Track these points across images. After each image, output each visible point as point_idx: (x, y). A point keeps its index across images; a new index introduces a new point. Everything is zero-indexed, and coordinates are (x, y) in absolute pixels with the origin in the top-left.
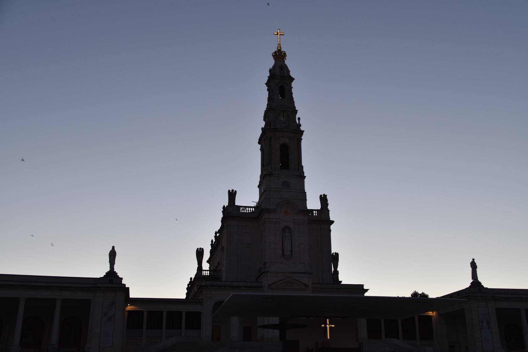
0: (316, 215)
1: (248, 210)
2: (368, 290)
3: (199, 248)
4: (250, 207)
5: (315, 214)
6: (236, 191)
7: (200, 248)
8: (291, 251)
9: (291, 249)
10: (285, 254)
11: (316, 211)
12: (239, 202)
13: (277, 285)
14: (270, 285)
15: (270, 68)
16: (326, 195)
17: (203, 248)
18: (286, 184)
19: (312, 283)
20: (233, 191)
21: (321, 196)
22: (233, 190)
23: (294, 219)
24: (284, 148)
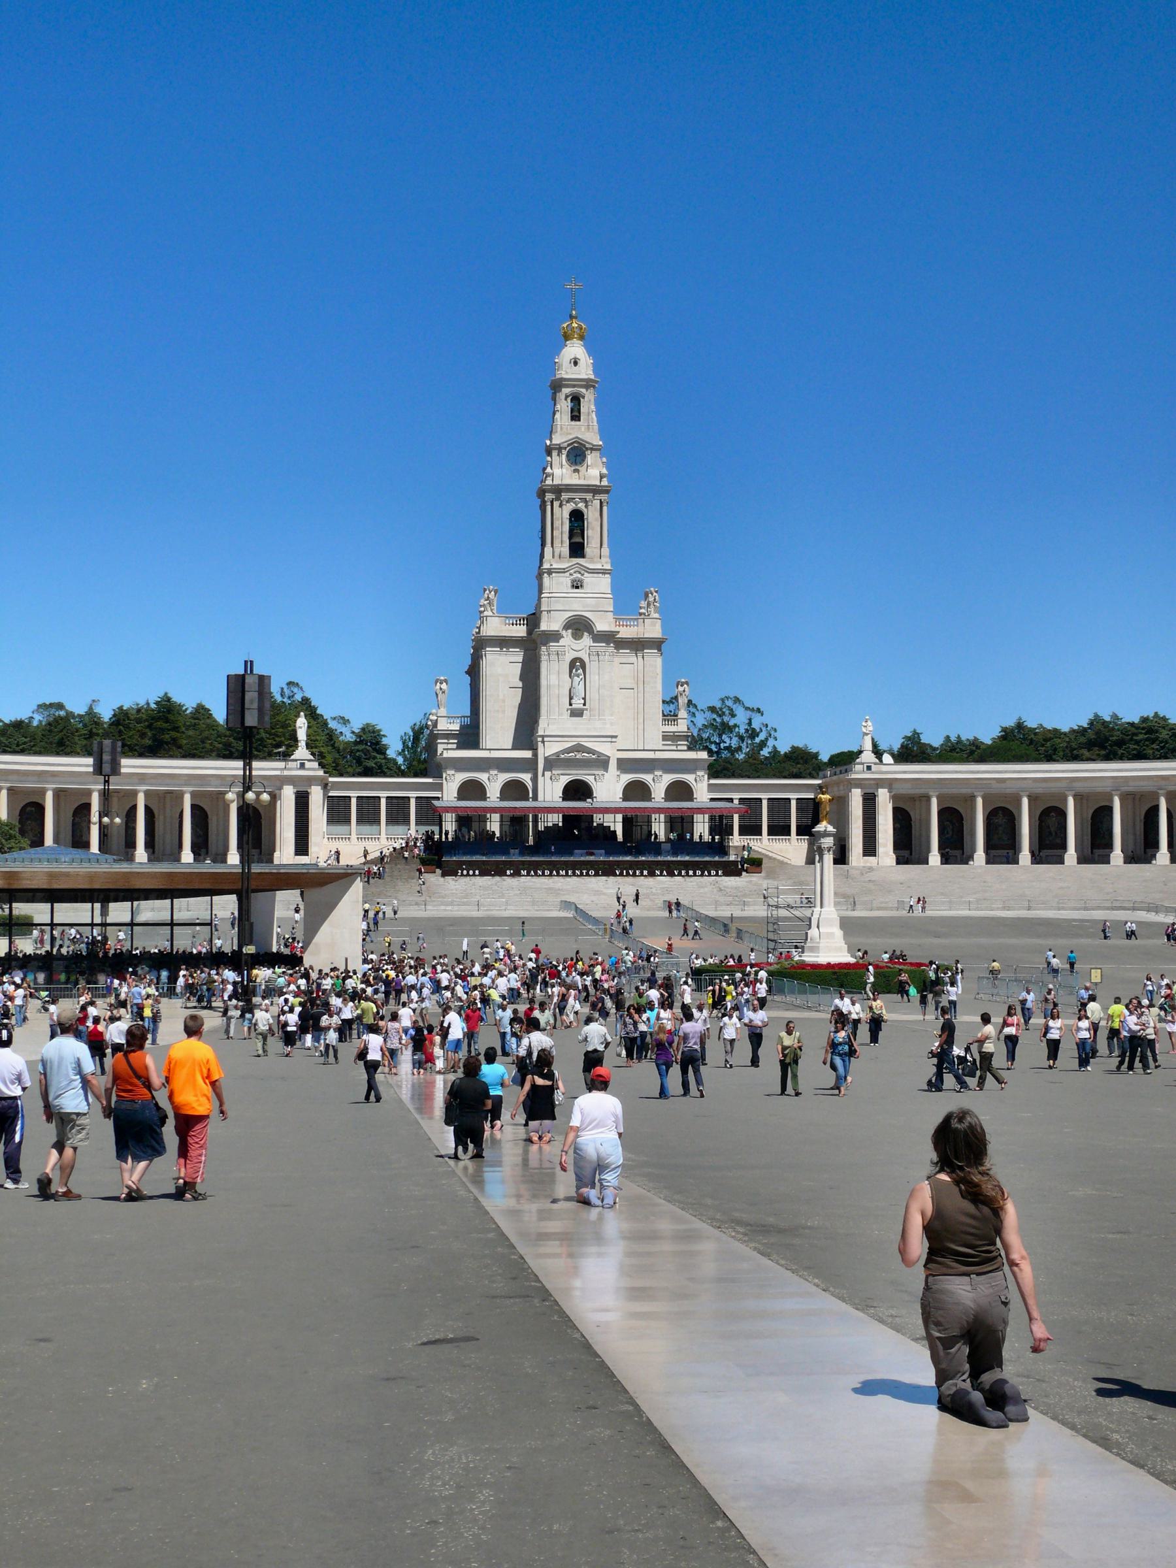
8: (584, 699)
18: (577, 585)
24: (577, 517)
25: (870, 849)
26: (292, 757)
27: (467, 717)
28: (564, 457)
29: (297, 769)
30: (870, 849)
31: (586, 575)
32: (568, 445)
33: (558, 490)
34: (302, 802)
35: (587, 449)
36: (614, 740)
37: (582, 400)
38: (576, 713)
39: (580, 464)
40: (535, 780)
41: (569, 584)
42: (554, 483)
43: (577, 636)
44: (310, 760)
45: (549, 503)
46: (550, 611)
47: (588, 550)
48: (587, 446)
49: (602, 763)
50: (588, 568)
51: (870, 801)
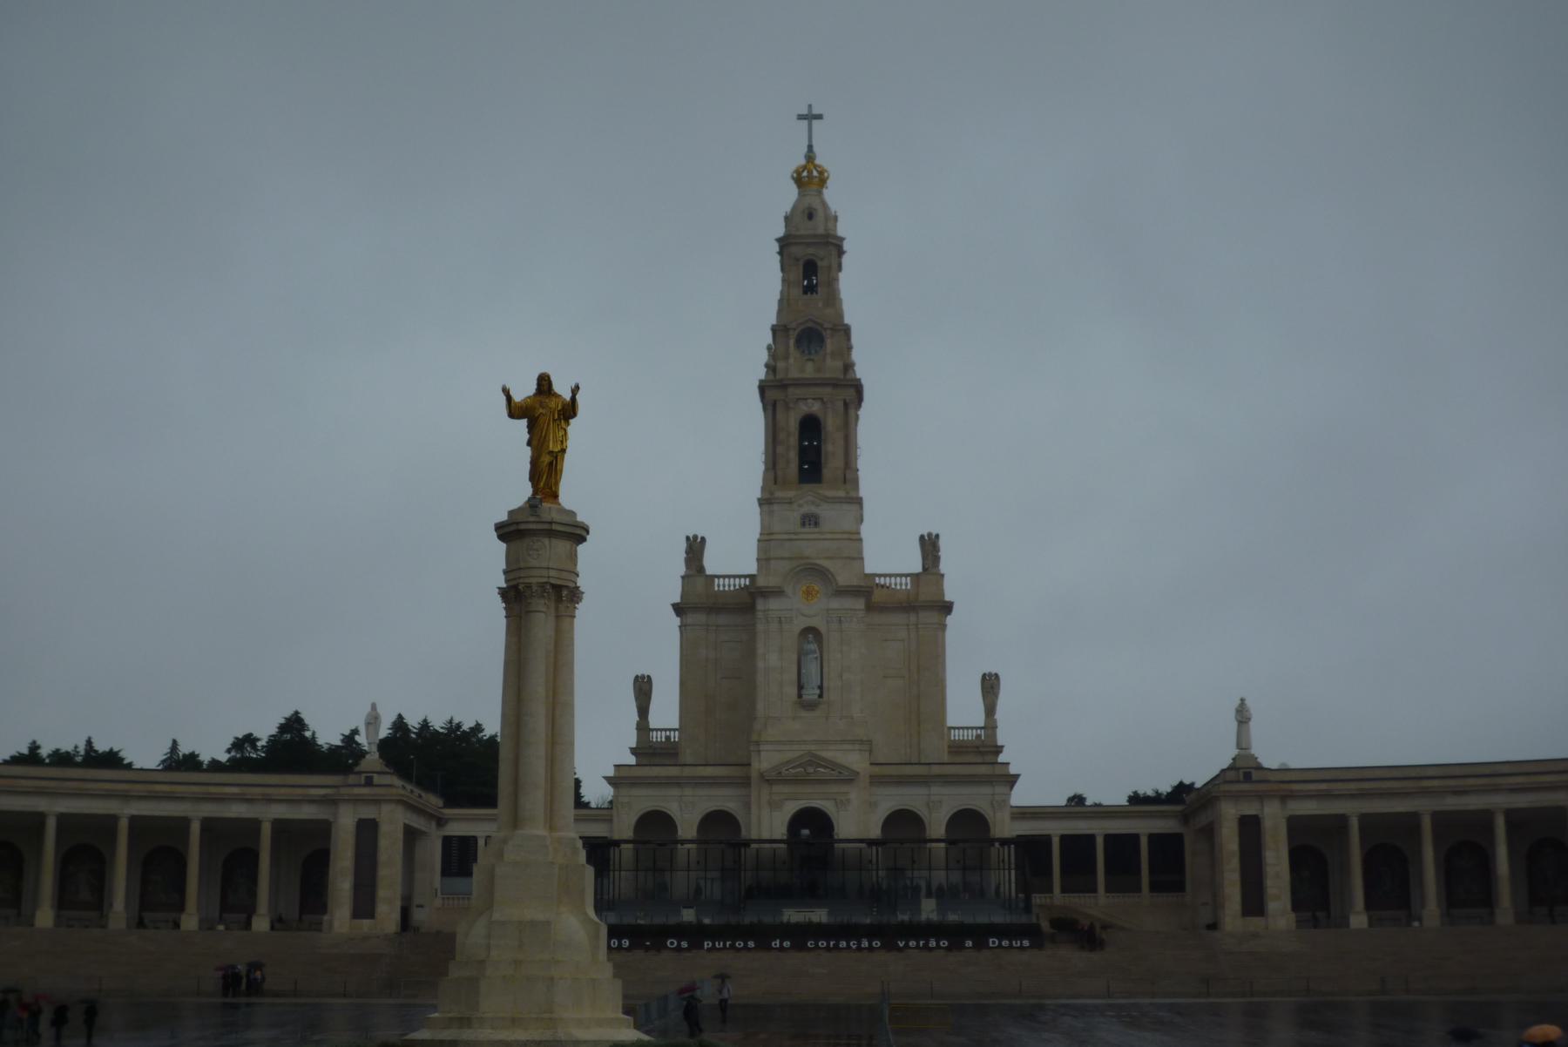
0: (909, 587)
1: (735, 586)
4: (740, 577)
5: (906, 584)
6: (703, 539)
7: (643, 677)
8: (821, 687)
9: (819, 683)
11: (909, 578)
12: (712, 564)
16: (937, 536)
17: (649, 677)
18: (810, 520)
21: (922, 537)
22: (695, 537)
23: (828, 610)
24: (811, 427)
25: (1254, 903)
26: (357, 769)
27: (675, 730)
28: (792, 342)
29: (359, 786)
30: (1254, 903)
33: (783, 386)
34: (367, 831)
35: (825, 329)
37: (819, 263)
38: (810, 706)
40: (747, 806)
42: (778, 377)
43: (809, 593)
44: (378, 773)
47: (827, 472)
48: (826, 325)
49: (849, 777)
50: (828, 498)
51: (1250, 828)
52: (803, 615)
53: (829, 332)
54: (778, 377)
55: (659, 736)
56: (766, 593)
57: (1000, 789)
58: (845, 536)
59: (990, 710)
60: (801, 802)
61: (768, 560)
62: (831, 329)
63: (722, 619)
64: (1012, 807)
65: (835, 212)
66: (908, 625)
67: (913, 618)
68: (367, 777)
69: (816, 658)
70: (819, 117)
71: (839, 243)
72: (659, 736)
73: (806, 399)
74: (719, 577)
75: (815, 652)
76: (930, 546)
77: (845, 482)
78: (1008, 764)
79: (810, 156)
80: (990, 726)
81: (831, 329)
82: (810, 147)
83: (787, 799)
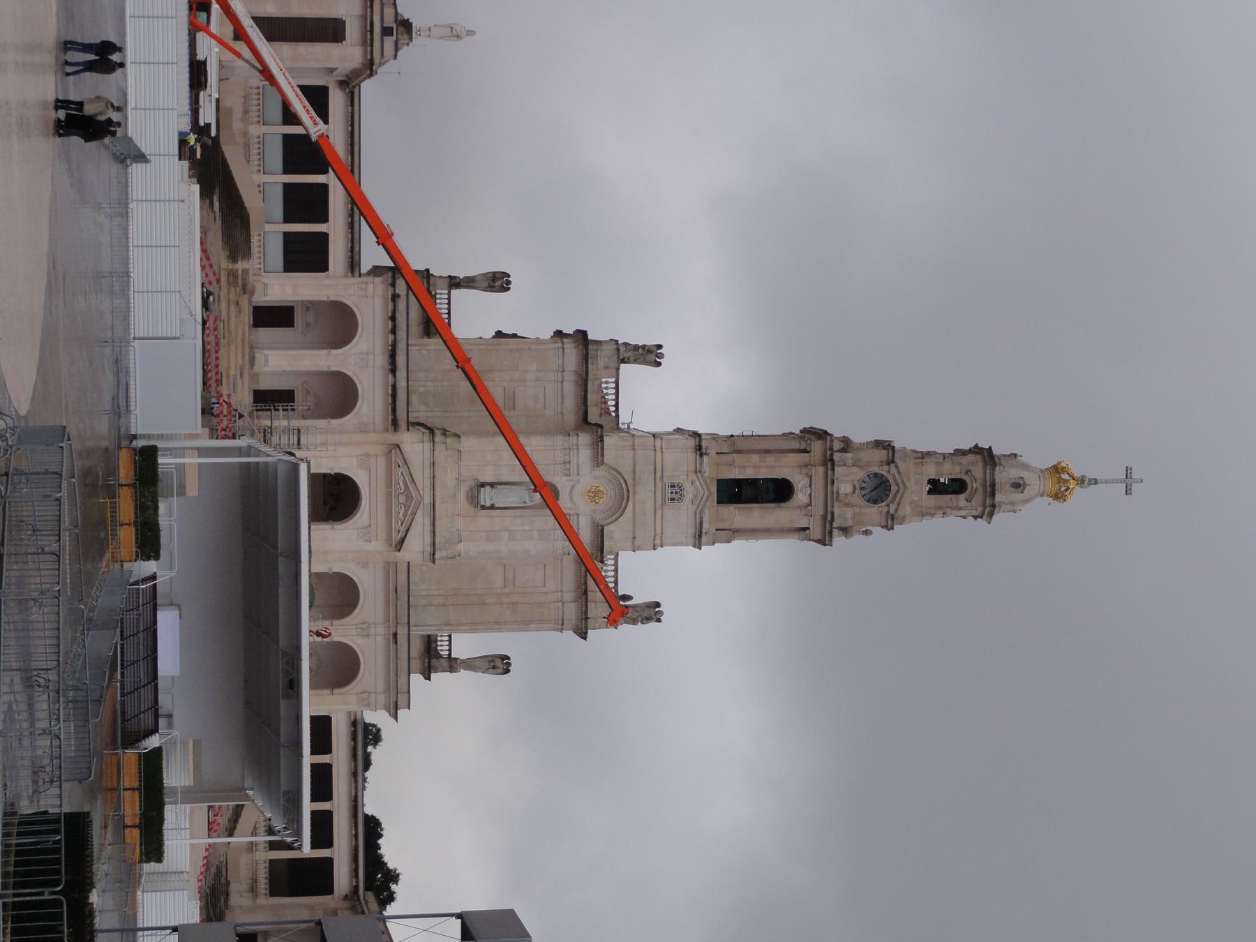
2: (396, 718)
3: (509, 279)
4: (617, 406)
6: (659, 364)
7: (509, 282)
8: (492, 507)
9: (497, 506)
10: (482, 489)
12: (629, 372)
13: (399, 466)
14: (398, 446)
15: (1021, 456)
16: (659, 620)
17: (509, 289)
19: (409, 563)
20: (658, 358)
21: (658, 605)
23: (578, 515)
24: (780, 491)
31: (692, 509)
32: (894, 475)
33: (829, 462)
35: (888, 505)
36: (427, 555)
37: (962, 497)
39: (863, 496)
40: (363, 430)
41: (676, 482)
42: (836, 457)
43: (595, 494)
45: (803, 446)
46: (634, 449)
52: (572, 487)
53: (885, 509)
54: (835, 454)
55: (442, 296)
56: (598, 444)
57: (381, 698)
58: (659, 531)
59: (470, 664)
60: (367, 490)
61: (634, 449)
62: (888, 512)
63: (570, 389)
64: (362, 712)
65: (1020, 510)
66: (561, 591)
67: (569, 596)
68: (392, 28)
69: (525, 502)
70: (1128, 491)
71: (984, 518)
72: (442, 296)
73: (810, 486)
74: (617, 383)
75: (531, 502)
76: (651, 612)
77: (717, 530)
78: (409, 708)
79: (1081, 481)
80: (453, 665)
81: (888, 512)
82: (1096, 482)
83: (370, 472)
